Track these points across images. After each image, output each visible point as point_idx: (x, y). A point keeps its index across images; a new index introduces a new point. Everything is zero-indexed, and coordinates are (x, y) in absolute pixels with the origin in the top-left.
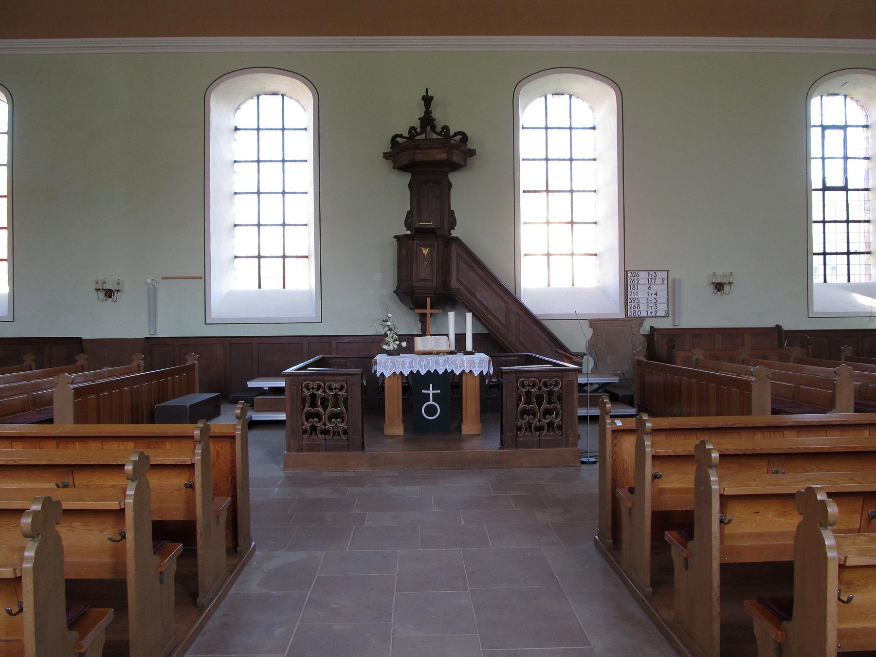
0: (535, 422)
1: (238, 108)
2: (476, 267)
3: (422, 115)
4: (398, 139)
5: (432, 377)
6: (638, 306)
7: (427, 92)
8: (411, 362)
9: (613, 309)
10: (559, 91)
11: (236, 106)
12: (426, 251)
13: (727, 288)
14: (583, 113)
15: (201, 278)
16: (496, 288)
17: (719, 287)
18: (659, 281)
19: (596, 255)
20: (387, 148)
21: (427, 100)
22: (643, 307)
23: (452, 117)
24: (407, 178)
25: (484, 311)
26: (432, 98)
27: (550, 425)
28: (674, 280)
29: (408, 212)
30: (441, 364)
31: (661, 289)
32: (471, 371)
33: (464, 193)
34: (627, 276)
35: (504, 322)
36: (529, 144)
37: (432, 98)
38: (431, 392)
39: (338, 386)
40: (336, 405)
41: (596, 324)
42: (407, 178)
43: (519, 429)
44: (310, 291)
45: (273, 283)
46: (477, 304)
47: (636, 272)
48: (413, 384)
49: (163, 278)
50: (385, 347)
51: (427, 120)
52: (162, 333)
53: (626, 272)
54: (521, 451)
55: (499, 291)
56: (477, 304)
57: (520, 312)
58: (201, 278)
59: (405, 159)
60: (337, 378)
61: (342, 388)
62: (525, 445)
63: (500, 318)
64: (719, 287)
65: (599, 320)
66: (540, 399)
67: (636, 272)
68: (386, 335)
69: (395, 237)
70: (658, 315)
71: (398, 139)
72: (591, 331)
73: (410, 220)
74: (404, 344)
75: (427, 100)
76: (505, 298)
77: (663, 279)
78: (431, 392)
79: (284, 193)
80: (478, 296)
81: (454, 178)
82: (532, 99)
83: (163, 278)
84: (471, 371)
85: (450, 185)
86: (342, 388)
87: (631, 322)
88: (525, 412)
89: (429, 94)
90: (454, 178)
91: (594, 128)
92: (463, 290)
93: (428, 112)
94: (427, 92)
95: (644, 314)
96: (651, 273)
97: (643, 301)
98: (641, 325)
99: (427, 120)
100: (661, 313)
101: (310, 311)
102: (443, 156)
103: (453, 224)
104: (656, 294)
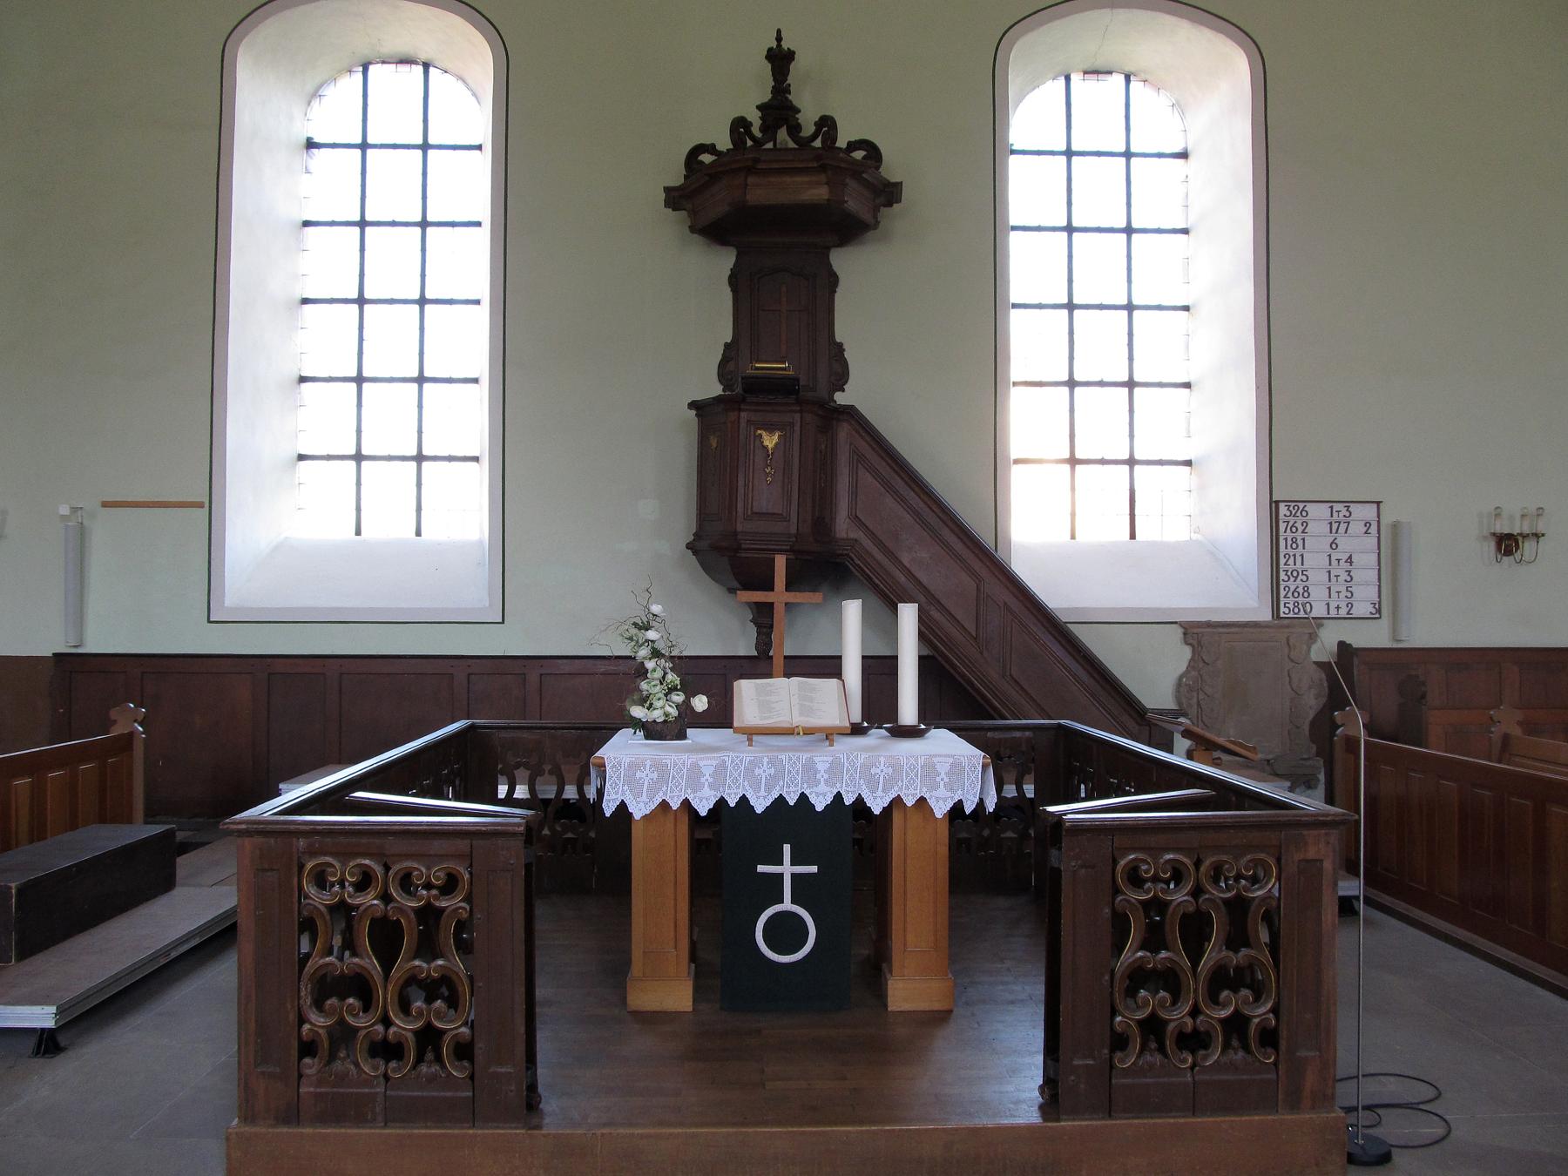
0: (1177, 1016)
1: (316, 94)
2: (900, 485)
3: (766, 96)
4: (707, 158)
5: (790, 818)
6: (1306, 589)
7: (779, 39)
8: (721, 769)
9: (1239, 597)
10: (1099, 64)
11: (310, 88)
12: (770, 441)
13: (1528, 547)
14: (1157, 120)
15: (201, 505)
16: (952, 539)
17: (1507, 544)
18: (1357, 527)
19: (1188, 463)
20: (676, 177)
21: (780, 59)
22: (1318, 595)
23: (847, 98)
24: (724, 261)
26: (790, 56)
27: (1236, 1025)
28: (1395, 526)
29: (726, 345)
30: (822, 775)
31: (1361, 547)
32: (922, 800)
34: (1278, 516)
35: (972, 629)
36: (1029, 190)
37: (790, 56)
38: (787, 869)
39: (438, 876)
40: (427, 947)
41: (1200, 635)
42: (724, 261)
43: (1119, 1042)
44: (481, 542)
45: (388, 521)
46: (903, 579)
47: (1299, 506)
48: (725, 841)
49: (105, 505)
50: (638, 712)
51: (779, 110)
52: (96, 644)
53: (1275, 505)
54: (1126, 1125)
55: (958, 546)
56: (903, 579)
58: (201, 505)
59: (718, 203)
60: (438, 846)
61: (450, 885)
62: (1142, 1104)
64: (1507, 544)
65: (1209, 624)
66: (1195, 930)
67: (1299, 506)
68: (642, 672)
69: (693, 405)
70: (1356, 612)
71: (707, 158)
72: (1187, 653)
73: (731, 366)
74: (700, 703)
75: (780, 59)
76: (977, 565)
77: (1368, 524)
78: (787, 869)
79: (422, 301)
80: (906, 559)
81: (844, 261)
82: (1034, 83)
83: (105, 505)
84: (922, 800)
85: (833, 281)
86: (450, 885)
87: (1286, 628)
88: (1139, 977)
89: (785, 45)
90: (844, 261)
91: (1184, 155)
92: (867, 543)
94: (779, 39)
95: (1319, 611)
96: (1337, 507)
97: (1317, 577)
98: (1313, 637)
99: (779, 110)
100: (1363, 608)
101: (473, 592)
102: (818, 192)
103: (840, 378)
104: (1350, 560)
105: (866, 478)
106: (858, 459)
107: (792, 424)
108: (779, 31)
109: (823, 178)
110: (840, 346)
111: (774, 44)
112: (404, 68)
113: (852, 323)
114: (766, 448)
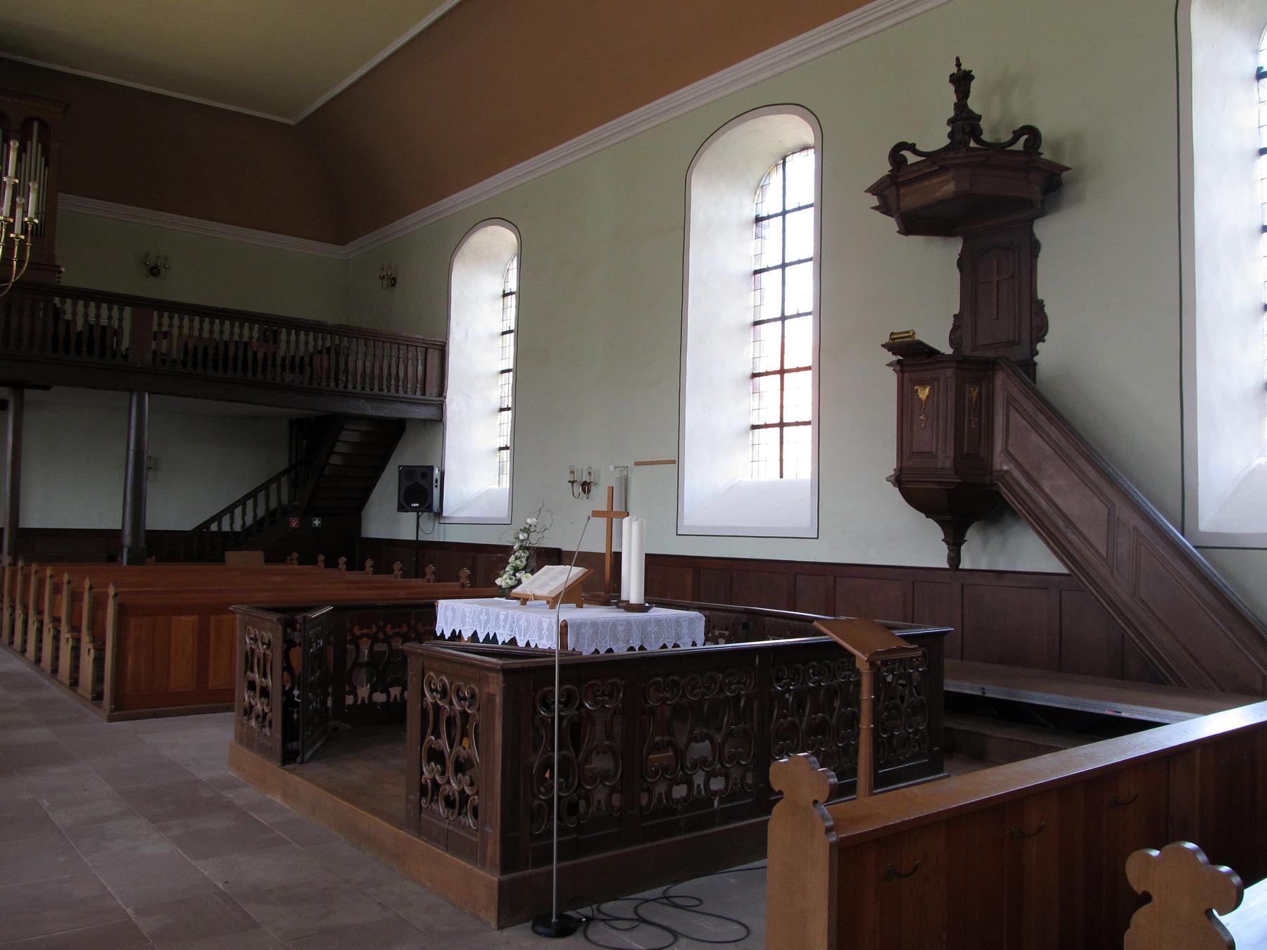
3: (951, 113)
7: (959, 65)
11: (753, 183)
15: (674, 462)
16: (1088, 469)
21: (962, 81)
25: (1061, 524)
33: (1070, 261)
35: (1104, 554)
46: (1044, 504)
49: (637, 464)
56: (1044, 504)
57: (1143, 527)
58: (674, 462)
63: (1092, 538)
75: (962, 81)
76: (1108, 491)
80: (1046, 487)
81: (1047, 230)
83: (637, 464)
85: (1034, 248)
92: (1017, 474)
93: (961, 106)
94: (959, 65)
99: (965, 122)
101: (800, 517)
103: (1039, 329)
105: (1015, 416)
106: (1010, 402)
107: (937, 379)
108: (958, 59)
109: (950, 175)
110: (1041, 305)
111: (955, 70)
112: (804, 153)
113: (1054, 283)
114: (920, 400)
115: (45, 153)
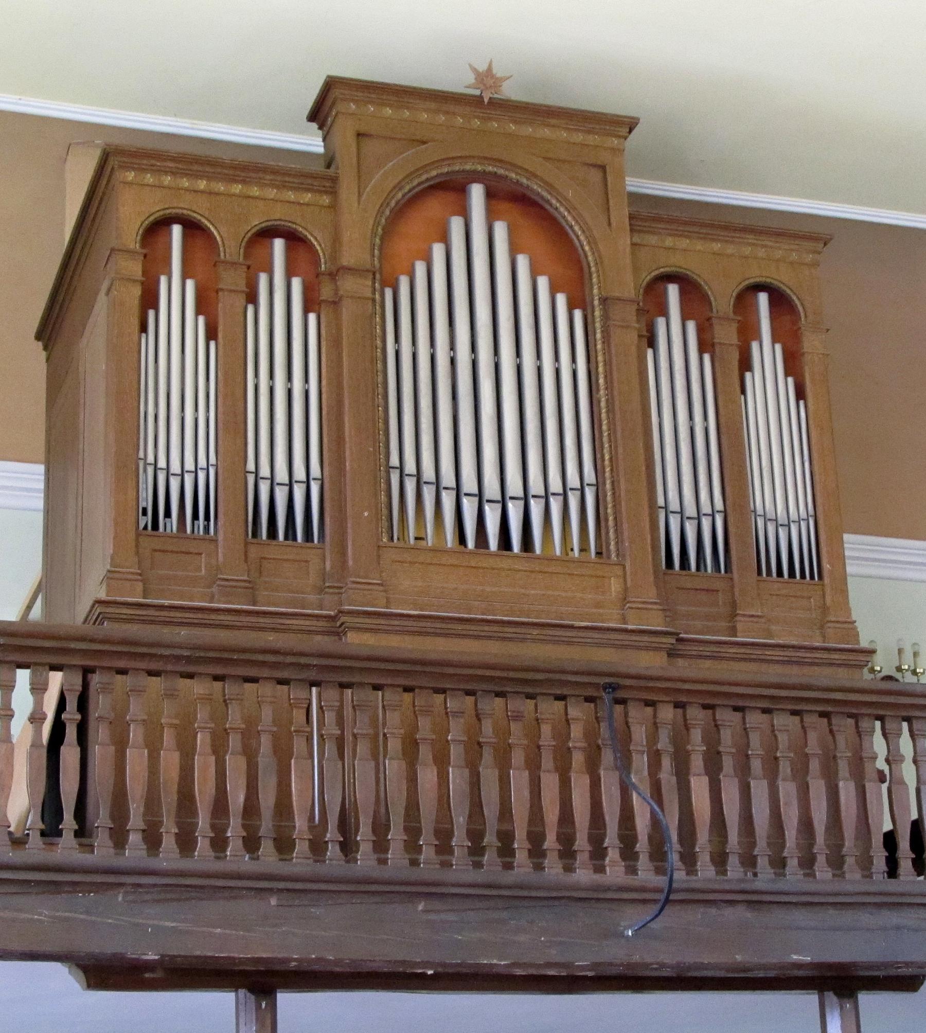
115: (793, 364)
